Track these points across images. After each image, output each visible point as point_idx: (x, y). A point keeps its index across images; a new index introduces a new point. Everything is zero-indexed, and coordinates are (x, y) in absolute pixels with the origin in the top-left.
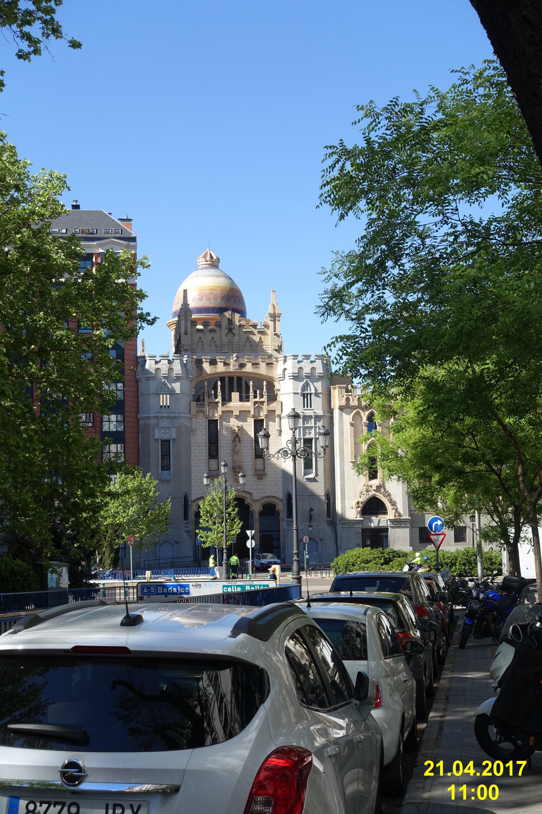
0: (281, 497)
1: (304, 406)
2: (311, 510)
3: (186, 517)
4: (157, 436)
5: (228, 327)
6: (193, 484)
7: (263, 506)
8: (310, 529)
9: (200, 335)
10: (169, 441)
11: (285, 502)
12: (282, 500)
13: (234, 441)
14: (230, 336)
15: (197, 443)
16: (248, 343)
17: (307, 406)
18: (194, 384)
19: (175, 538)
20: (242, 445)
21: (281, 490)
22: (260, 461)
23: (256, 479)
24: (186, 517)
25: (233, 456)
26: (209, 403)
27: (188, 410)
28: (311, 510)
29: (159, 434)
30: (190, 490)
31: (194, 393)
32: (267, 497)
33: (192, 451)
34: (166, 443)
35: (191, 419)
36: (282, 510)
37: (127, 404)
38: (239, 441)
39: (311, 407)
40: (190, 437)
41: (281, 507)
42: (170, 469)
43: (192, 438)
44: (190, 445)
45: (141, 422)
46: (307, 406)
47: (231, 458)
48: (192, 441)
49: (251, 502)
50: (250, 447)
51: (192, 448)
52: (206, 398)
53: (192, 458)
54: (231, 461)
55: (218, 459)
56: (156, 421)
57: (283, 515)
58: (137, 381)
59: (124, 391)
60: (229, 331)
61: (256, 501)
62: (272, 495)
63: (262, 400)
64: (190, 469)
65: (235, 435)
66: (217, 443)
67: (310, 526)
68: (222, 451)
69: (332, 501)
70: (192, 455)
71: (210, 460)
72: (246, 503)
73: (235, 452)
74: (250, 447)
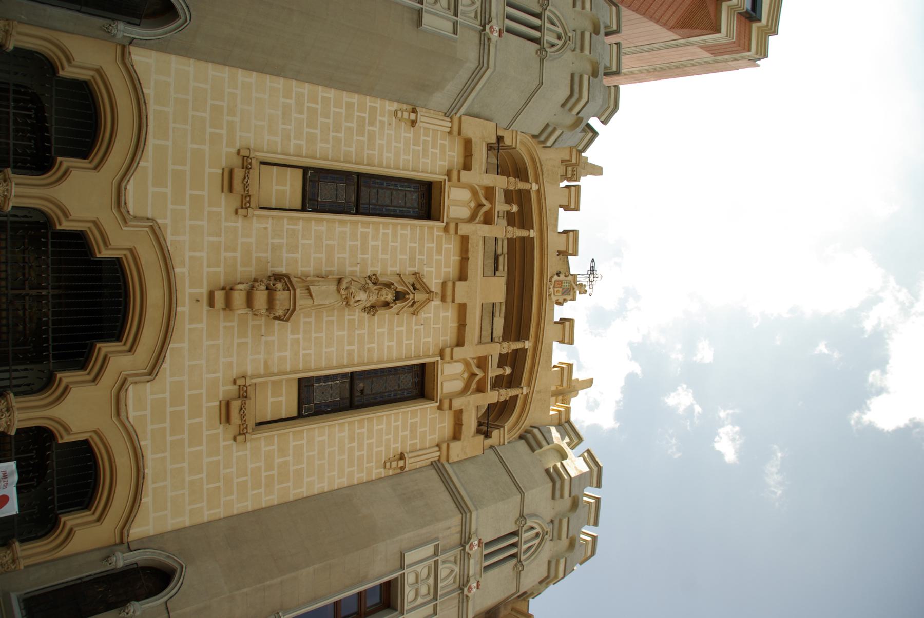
0: (137, 531)
1: (488, 544)
6: (212, 71)
7: (86, 442)
11: (121, 560)
13: (374, 280)
15: (372, 124)
17: (487, 556)
21: (172, 522)
22: (287, 402)
23: (226, 389)
25: (322, 277)
30: (186, 51)
33: (346, 97)
35: (448, 115)
36: (73, 547)
38: (372, 309)
39: (487, 568)
40: (393, 100)
44: (369, 92)
46: (487, 556)
48: (378, 103)
49: (109, 378)
50: (350, 353)
51: (355, 98)
53: (321, 92)
55: (304, 209)
61: (118, 404)
62: (150, 486)
64: (278, 72)
65: (400, 288)
66: (358, 209)
68: (338, 229)
70: (331, 94)
71: (300, 172)
72: (104, 347)
74: (350, 353)
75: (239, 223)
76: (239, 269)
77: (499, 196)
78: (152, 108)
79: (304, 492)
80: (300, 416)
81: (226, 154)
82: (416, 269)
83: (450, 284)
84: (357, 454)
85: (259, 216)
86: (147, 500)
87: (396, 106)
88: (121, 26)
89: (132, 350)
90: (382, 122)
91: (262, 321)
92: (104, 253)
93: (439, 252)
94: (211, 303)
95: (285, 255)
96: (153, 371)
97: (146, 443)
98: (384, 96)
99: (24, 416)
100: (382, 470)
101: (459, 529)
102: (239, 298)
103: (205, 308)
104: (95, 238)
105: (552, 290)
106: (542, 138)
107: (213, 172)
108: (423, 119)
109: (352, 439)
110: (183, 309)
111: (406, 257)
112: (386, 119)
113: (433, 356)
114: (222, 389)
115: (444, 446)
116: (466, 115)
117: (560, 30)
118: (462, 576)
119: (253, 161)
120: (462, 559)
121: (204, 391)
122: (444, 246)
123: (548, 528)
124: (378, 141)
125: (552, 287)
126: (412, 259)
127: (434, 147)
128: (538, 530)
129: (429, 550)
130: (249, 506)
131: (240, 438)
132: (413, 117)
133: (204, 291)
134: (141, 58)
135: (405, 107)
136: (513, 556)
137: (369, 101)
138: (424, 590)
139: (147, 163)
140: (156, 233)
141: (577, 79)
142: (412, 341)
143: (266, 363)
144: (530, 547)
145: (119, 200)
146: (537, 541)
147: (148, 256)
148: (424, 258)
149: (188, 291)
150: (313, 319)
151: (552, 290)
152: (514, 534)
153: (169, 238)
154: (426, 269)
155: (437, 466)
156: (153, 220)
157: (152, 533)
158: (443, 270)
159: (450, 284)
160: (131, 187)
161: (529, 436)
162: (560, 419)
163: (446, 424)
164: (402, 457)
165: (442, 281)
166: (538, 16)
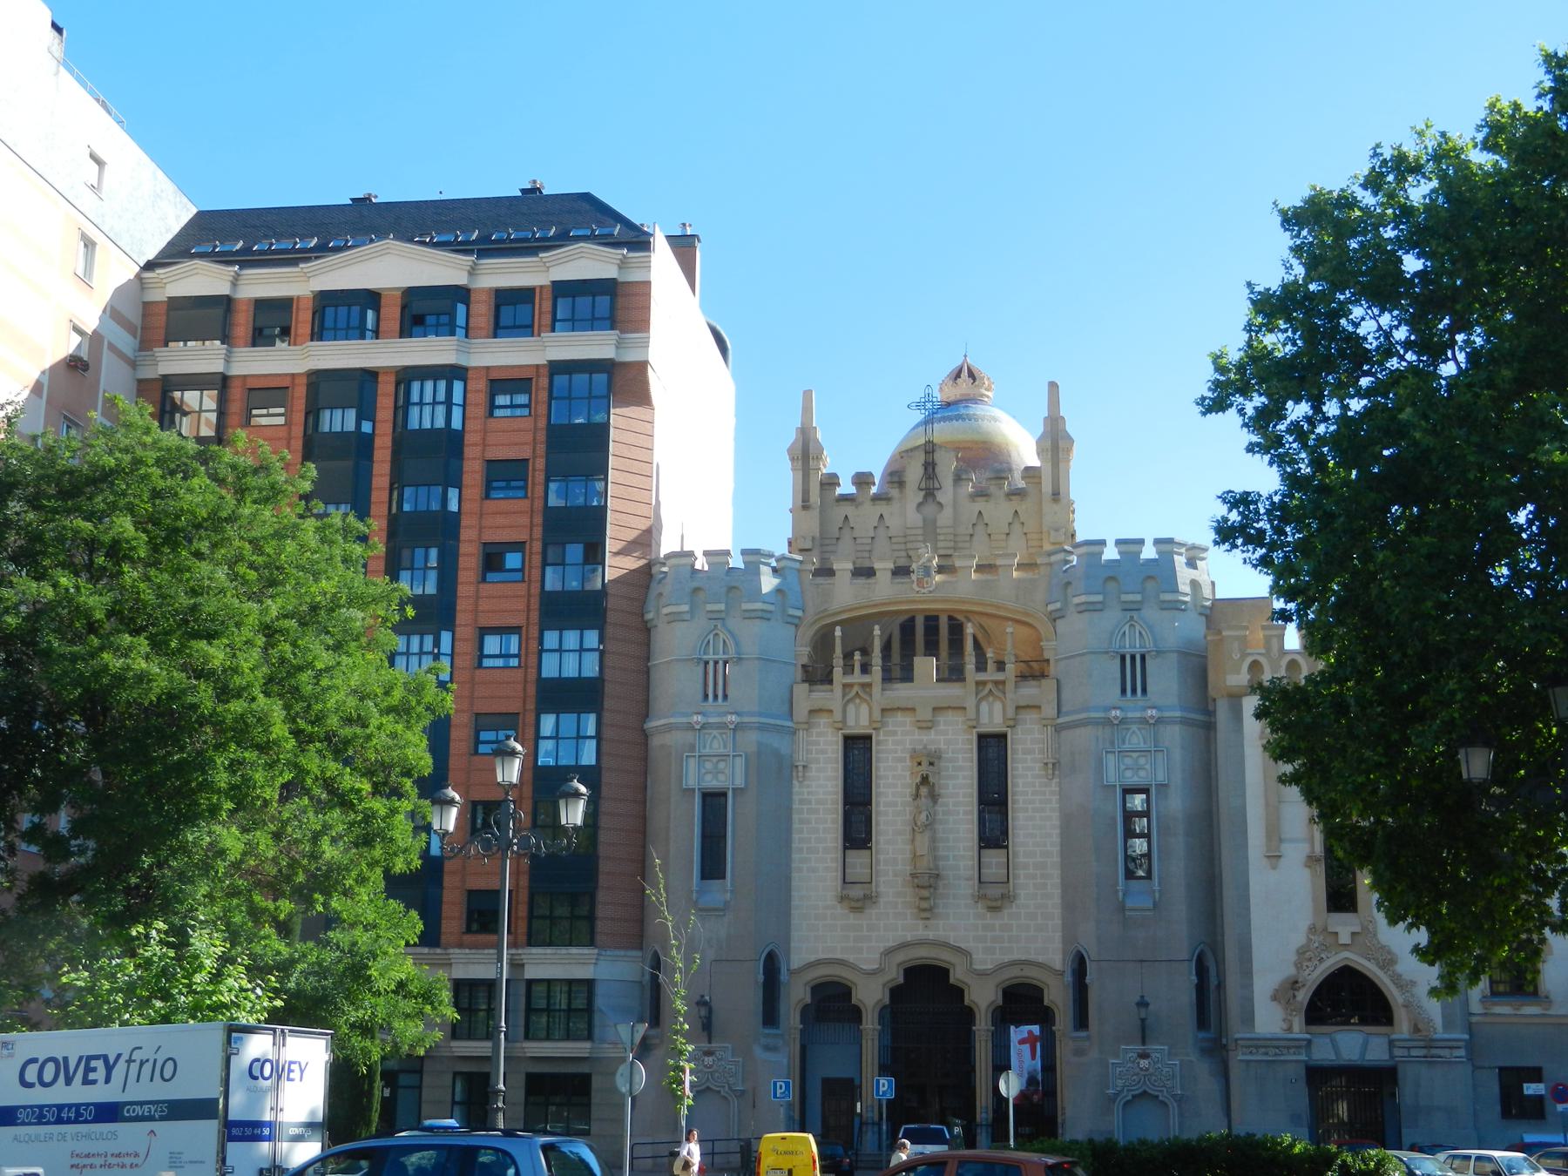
0: (1058, 965)
1: (1124, 691)
2: (1142, 1004)
3: (770, 1016)
4: (692, 781)
5: (923, 485)
8: (1144, 1063)
9: (848, 509)
10: (724, 795)
11: (1069, 978)
12: (1062, 973)
13: (917, 796)
14: (930, 509)
15: (810, 802)
16: (980, 528)
17: (1134, 691)
18: (808, 633)
19: (732, 1080)
20: (939, 809)
23: (980, 908)
24: (770, 1016)
25: (913, 841)
26: (845, 686)
27: (786, 708)
28: (1142, 1004)
29: (699, 776)
31: (805, 660)
32: (1013, 963)
33: (796, 826)
34: (713, 803)
35: (794, 732)
37: (609, 688)
41: (1058, 996)
42: (724, 877)
43: (796, 789)
44: (789, 809)
45: (656, 741)
46: (1134, 691)
47: (908, 847)
48: (796, 798)
50: (966, 813)
51: (795, 817)
52: (838, 672)
54: (908, 856)
56: (689, 737)
57: (1063, 1020)
58: (646, 630)
59: (602, 653)
60: (925, 497)
61: (982, 974)
62: (1032, 957)
63: (1000, 676)
65: (918, 780)
66: (868, 802)
67: (1144, 1056)
68: (882, 827)
69: (1213, 982)
72: (952, 981)
73: (925, 826)
75: (882, 900)
76: (908, 899)
77: (848, 680)
78: (821, 956)
79: (1056, 850)
80: (1007, 847)
81: (840, 910)
82: (908, 756)
83: (919, 724)
84: (1038, 805)
85: (877, 886)
86: (1040, 959)
87: (795, 782)
88: (782, 978)
89: (953, 965)
90: (809, 793)
91: (941, 883)
92: (901, 980)
93: (894, 733)
94: (928, 919)
95: (900, 867)
96: (965, 953)
97: (1007, 958)
98: (790, 794)
99: (983, 1024)
100: (1054, 780)
101: (1100, 727)
102: (925, 905)
103: (931, 921)
104: (894, 984)
105: (925, 591)
106: (796, 621)
107: (853, 919)
108: (801, 758)
109: (1026, 810)
110: (931, 935)
111: (899, 765)
112: (805, 790)
113: (972, 734)
114: (980, 910)
115: (1044, 722)
116: (792, 715)
117: (711, 636)
118: (1141, 723)
119: (844, 892)
120: (1125, 723)
121: (980, 922)
122: (890, 728)
123: (1128, 614)
124: (821, 796)
125: (923, 591)
126: (901, 760)
127: (818, 743)
128: (1127, 628)
129: (1111, 760)
130: (1057, 892)
131: (1012, 899)
132: (800, 768)
133: (921, 922)
134: (797, 961)
135: (794, 774)
136: (1143, 658)
137: (796, 806)
138: (1142, 761)
139: (851, 958)
140: (889, 952)
141: (747, 615)
142: (960, 756)
143: (967, 879)
144: (1140, 633)
145: (873, 973)
146: (1138, 627)
147: (901, 957)
148: (899, 747)
149: (920, 932)
150: (941, 845)
151: (925, 591)
152: (1123, 658)
153: (891, 944)
154: (908, 746)
155: (1059, 729)
156: (881, 954)
157: (1061, 956)
158: (908, 728)
159: (919, 724)
160: (864, 967)
161: (1053, 616)
162: (1047, 564)
163: (1028, 717)
164: (1046, 764)
165: (917, 731)
166: (707, 663)
